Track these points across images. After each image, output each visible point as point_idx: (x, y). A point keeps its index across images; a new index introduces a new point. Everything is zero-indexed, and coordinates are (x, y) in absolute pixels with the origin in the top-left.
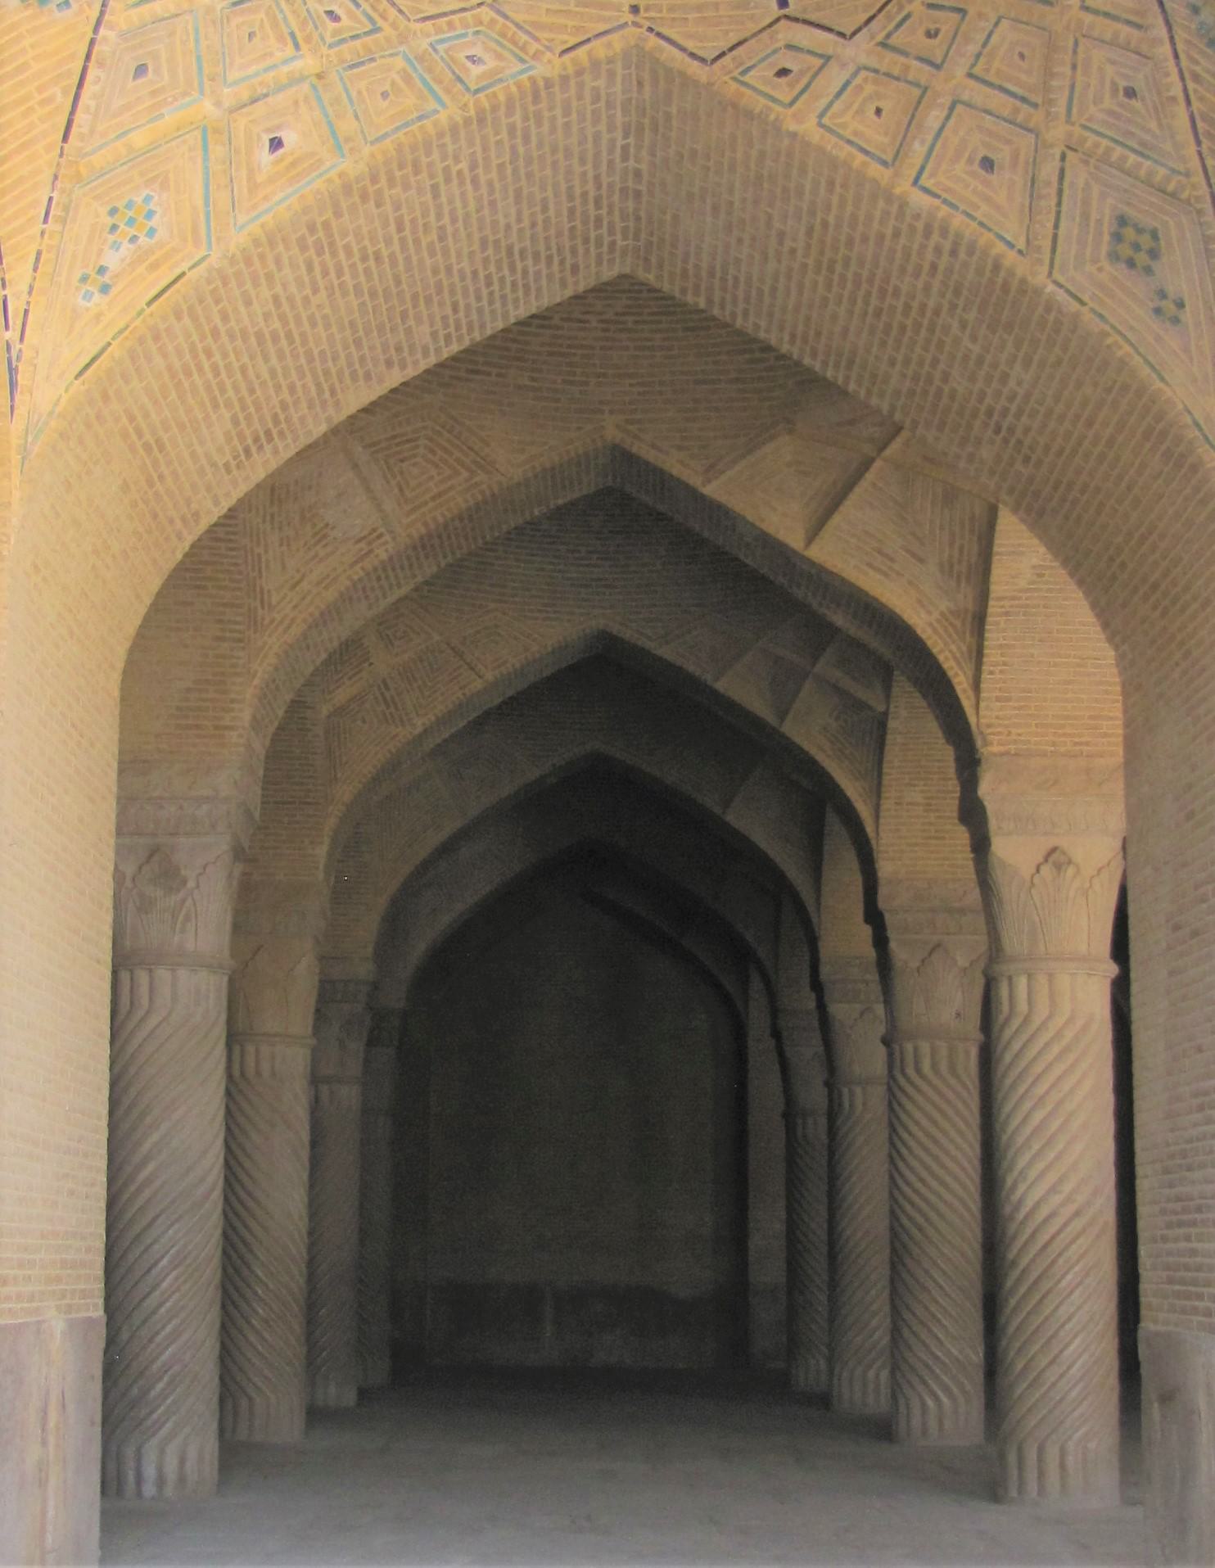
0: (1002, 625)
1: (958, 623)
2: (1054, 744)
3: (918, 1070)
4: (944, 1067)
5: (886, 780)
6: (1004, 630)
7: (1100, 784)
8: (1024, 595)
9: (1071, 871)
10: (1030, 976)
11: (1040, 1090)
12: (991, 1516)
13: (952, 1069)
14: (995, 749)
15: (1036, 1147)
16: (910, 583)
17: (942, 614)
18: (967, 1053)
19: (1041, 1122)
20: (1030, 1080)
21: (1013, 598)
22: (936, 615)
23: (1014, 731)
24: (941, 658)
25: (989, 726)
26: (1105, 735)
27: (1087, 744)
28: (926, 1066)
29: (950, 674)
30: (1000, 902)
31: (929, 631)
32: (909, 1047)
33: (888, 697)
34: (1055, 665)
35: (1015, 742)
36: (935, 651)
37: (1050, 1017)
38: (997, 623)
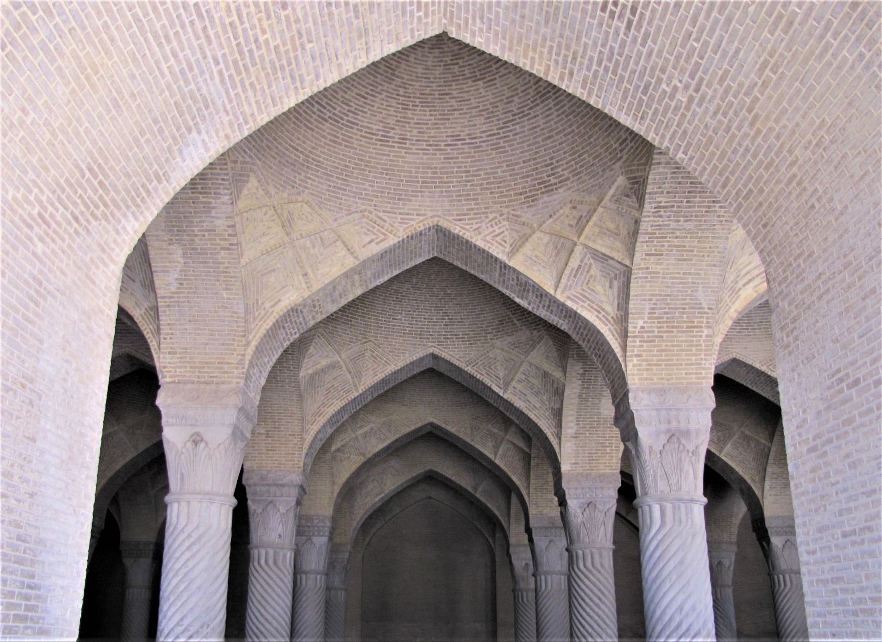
0: (168, 313)
2: (198, 377)
3: (259, 563)
4: (271, 562)
6: (169, 315)
7: (221, 399)
8: (176, 296)
9: (202, 445)
13: (275, 563)
14: (168, 380)
15: (172, 599)
16: (132, 294)
17: (146, 309)
18: (285, 556)
20: (173, 561)
21: (171, 297)
22: (143, 310)
24: (145, 333)
25: (165, 367)
26: (227, 372)
27: (216, 377)
28: (263, 562)
29: (149, 341)
31: (140, 318)
34: (199, 334)
35: (178, 376)
36: (142, 329)
38: (165, 311)
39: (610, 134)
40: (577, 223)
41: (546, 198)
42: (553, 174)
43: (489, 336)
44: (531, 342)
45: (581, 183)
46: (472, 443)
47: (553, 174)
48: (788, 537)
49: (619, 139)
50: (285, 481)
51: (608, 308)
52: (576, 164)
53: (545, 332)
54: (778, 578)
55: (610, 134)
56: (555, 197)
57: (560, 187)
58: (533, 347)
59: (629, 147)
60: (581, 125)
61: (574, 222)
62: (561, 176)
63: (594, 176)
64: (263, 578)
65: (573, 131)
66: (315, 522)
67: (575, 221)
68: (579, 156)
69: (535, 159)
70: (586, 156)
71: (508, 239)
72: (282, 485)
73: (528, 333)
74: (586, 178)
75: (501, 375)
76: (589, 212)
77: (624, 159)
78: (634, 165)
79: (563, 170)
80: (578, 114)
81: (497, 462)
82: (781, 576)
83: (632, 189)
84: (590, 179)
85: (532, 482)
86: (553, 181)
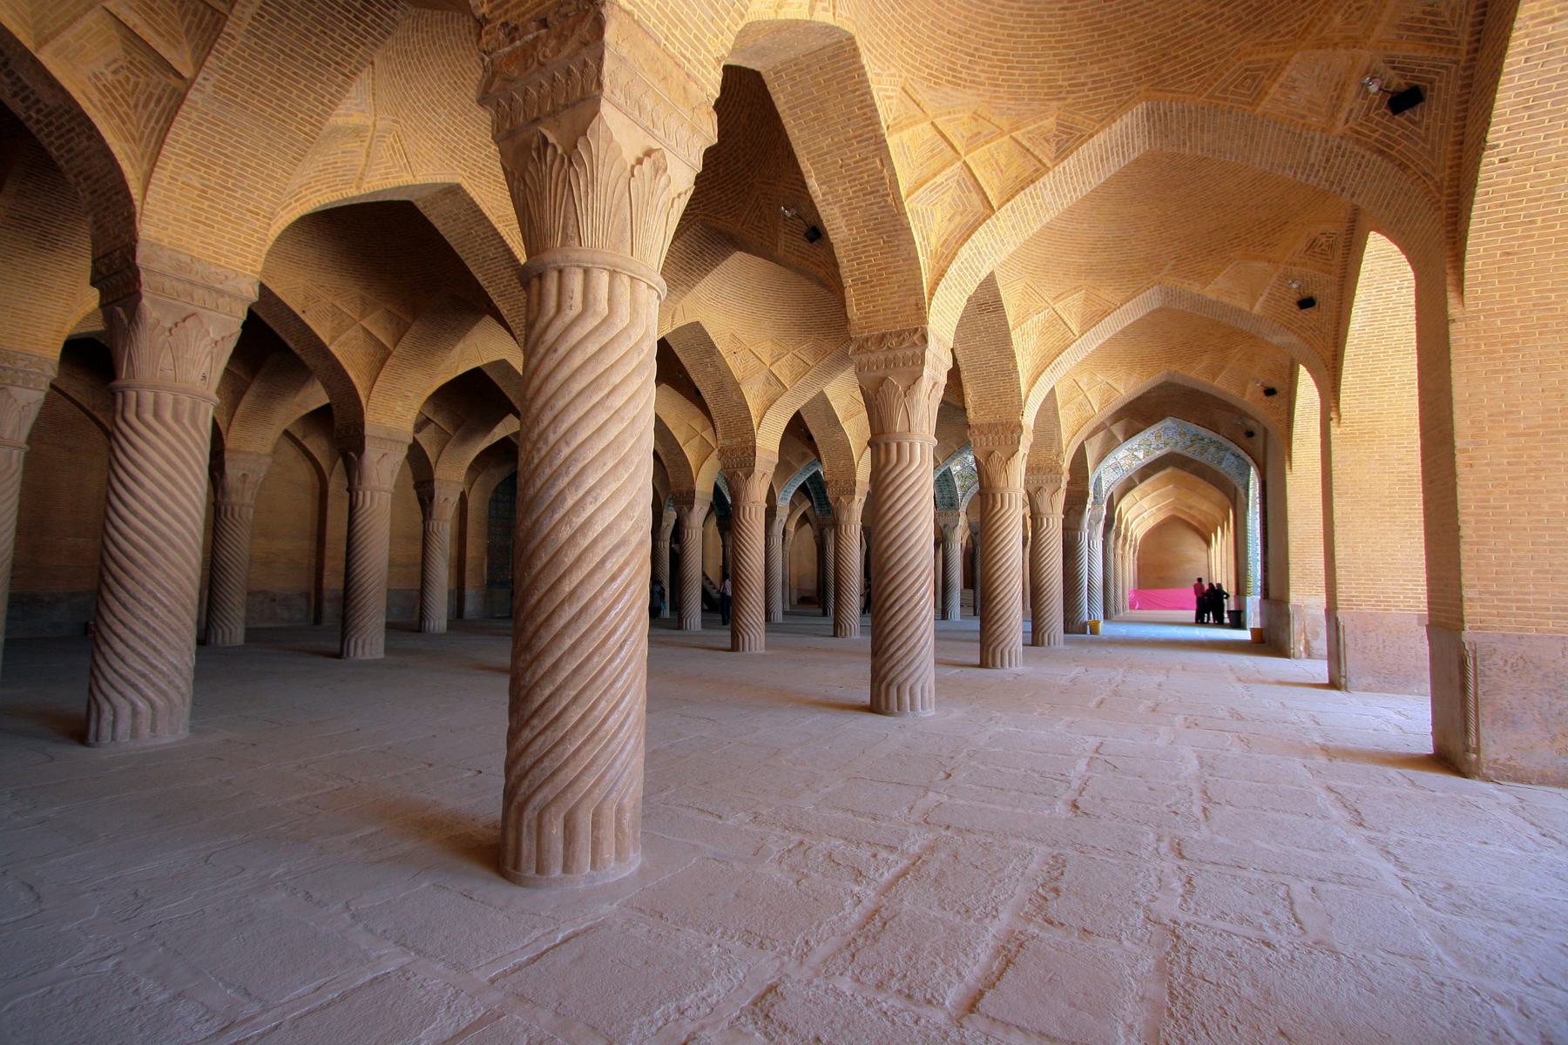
3: (157, 415)
5: (166, 150)
10: (613, 274)
11: (618, 401)
12: (498, 891)
28: (168, 416)
32: (148, 397)
33: (199, 65)
37: (632, 324)
41: (948, 89)
46: (302, 316)
50: (227, 286)
51: (933, 240)
61: (967, 134)
64: (167, 443)
66: (20, 364)
71: (894, 108)
72: (221, 293)
81: (332, 348)
85: (378, 383)
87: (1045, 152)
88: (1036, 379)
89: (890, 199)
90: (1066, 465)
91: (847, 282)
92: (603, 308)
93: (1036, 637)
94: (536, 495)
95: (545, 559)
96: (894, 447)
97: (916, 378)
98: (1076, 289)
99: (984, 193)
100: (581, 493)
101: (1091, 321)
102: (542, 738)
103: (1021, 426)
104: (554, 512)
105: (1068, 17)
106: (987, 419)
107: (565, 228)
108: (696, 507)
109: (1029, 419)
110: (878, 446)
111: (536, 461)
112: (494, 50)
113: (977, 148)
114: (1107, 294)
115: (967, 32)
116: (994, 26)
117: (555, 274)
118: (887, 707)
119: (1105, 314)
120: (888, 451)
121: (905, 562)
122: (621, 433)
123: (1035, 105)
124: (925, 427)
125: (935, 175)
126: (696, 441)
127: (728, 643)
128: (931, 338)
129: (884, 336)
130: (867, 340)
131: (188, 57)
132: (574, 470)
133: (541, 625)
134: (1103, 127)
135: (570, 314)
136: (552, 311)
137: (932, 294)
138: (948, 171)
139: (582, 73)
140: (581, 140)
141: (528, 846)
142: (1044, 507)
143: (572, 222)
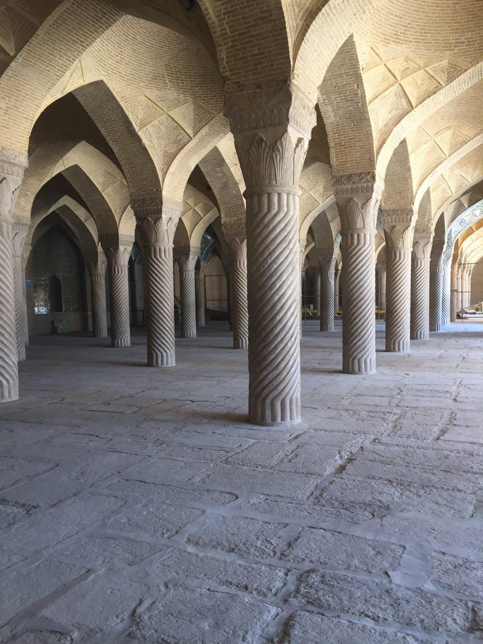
1: (297, 10)
10: (288, 194)
19: (292, 260)
23: (300, 76)
30: (282, 158)
33: (18, 50)
39: (453, 33)
40: (404, 71)
41: (393, 45)
42: (404, 33)
43: (142, 84)
44: (177, 102)
45: (418, 49)
47: (404, 33)
48: (126, 247)
49: (458, 39)
52: (420, 36)
53: (190, 100)
54: (114, 269)
55: (453, 33)
56: (399, 48)
57: (404, 44)
58: (177, 105)
59: (462, 48)
60: (439, 17)
62: (407, 37)
63: (428, 50)
65: (433, 17)
67: (403, 69)
68: (425, 33)
69: (401, 18)
70: (429, 35)
73: (175, 94)
74: (423, 48)
75: (140, 117)
76: (415, 68)
77: (454, 52)
78: (460, 59)
79: (411, 35)
80: (444, 10)
82: (120, 268)
83: (447, 69)
84: (424, 50)
86: (402, 38)
87: (442, 78)
88: (422, 182)
89: (360, 104)
90: (433, 228)
91: (332, 145)
92: (285, 209)
93: (414, 334)
94: (263, 284)
95: (269, 307)
96: (356, 236)
97: (368, 199)
98: (449, 128)
99: (409, 99)
100: (281, 282)
101: (457, 146)
102: (272, 374)
103: (412, 211)
104: (272, 290)
105: (457, 8)
106: (392, 207)
107: (270, 176)
108: (191, 257)
109: (416, 207)
110: (346, 235)
111: (262, 270)
112: (231, 93)
113: (407, 76)
114: (467, 131)
115: (404, 15)
116: (419, 12)
117: (266, 195)
118: (353, 370)
119: (464, 143)
120: (352, 239)
121: (362, 296)
122: (293, 258)
123: (438, 53)
124: (372, 226)
125: (384, 91)
126: (190, 213)
127: (231, 344)
128: (377, 177)
129: (351, 175)
130: (341, 177)
131: (13, 45)
132: (279, 274)
133: (269, 332)
134: (472, 66)
135: (274, 212)
136: (266, 210)
137: (378, 153)
138: (391, 89)
139: (279, 112)
140: (279, 141)
141: (268, 413)
142: (420, 255)
143: (273, 174)
